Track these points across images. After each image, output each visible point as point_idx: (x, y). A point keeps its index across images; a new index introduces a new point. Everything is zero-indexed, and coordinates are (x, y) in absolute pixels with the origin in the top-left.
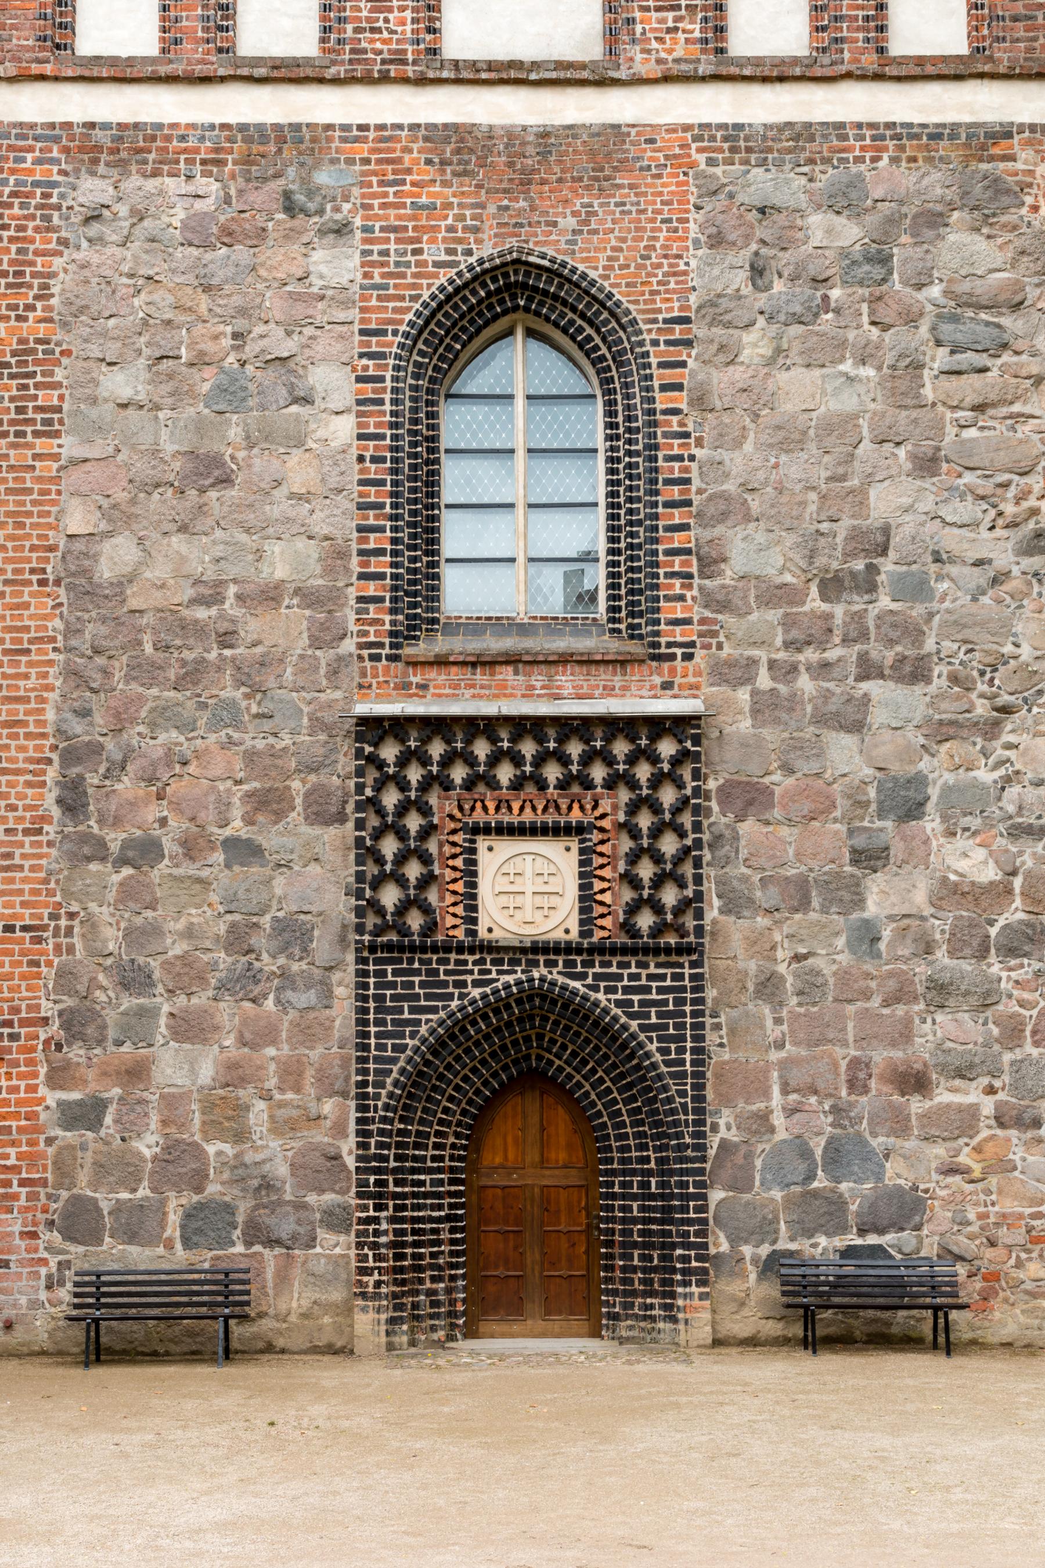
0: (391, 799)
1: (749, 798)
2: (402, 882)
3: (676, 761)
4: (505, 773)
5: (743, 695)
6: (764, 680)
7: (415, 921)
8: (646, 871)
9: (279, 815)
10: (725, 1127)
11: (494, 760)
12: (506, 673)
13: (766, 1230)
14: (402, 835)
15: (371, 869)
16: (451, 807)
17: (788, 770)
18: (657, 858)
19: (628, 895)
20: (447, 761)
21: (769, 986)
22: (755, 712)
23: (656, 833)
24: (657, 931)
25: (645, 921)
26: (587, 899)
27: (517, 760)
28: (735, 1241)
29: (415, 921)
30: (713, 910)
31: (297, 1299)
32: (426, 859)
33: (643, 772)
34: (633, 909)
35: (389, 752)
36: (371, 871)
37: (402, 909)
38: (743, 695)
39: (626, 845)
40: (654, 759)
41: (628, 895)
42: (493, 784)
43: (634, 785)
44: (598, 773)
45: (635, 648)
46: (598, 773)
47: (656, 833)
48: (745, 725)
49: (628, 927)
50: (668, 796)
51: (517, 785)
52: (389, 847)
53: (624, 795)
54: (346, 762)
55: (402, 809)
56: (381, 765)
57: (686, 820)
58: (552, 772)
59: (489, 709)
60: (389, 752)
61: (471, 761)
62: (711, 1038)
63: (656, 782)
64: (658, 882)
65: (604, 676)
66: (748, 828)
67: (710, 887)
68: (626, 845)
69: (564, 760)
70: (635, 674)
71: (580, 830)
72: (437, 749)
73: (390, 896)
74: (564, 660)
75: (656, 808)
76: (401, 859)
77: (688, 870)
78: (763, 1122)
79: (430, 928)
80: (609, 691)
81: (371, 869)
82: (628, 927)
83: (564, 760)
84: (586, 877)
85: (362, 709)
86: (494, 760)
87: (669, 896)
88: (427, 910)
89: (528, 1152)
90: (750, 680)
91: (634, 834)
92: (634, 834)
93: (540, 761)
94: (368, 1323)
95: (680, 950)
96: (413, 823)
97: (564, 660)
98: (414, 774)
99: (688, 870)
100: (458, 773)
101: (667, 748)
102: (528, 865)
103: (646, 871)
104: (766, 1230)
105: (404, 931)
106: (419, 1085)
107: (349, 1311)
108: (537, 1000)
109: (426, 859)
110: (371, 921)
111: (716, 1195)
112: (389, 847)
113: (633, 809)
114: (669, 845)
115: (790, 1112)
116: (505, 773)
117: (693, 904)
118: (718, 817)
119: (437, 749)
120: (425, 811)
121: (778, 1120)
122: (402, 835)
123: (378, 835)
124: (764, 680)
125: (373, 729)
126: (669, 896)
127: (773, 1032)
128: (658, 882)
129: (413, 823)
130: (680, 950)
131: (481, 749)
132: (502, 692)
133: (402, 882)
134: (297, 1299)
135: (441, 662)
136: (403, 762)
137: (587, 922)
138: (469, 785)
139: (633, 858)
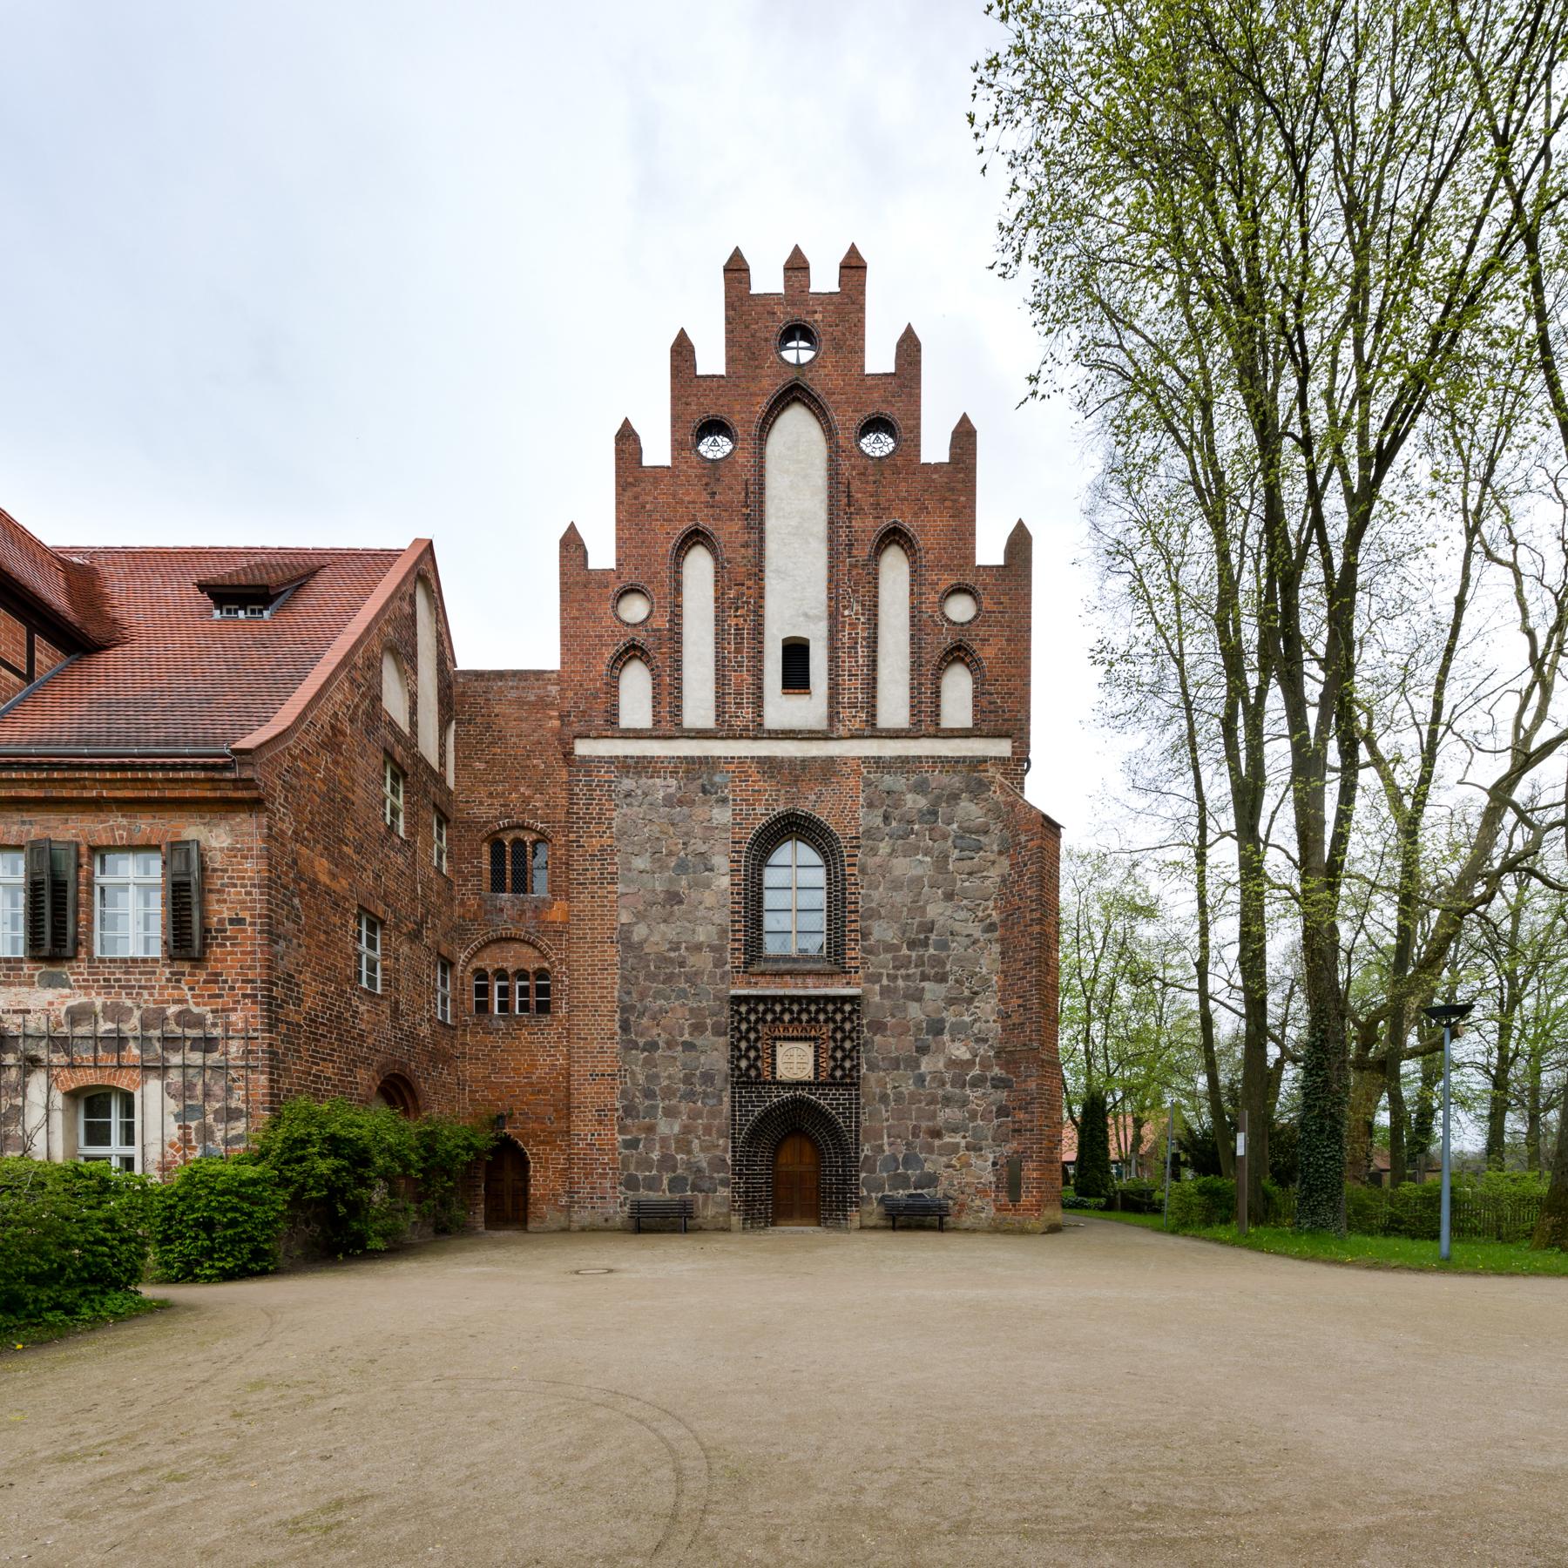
0: (744, 1027)
1: (878, 1027)
2: (748, 1058)
3: (851, 1013)
4: (787, 1017)
5: (877, 987)
6: (885, 982)
7: (753, 1073)
8: (839, 1055)
9: (702, 1033)
10: (866, 1150)
11: (782, 1012)
12: (788, 978)
13: (881, 1188)
14: (748, 1040)
15: (737, 1053)
16: (766, 1030)
17: (893, 1016)
18: (843, 1050)
19: (832, 1064)
20: (765, 1012)
21: (884, 1098)
22: (881, 994)
23: (843, 1040)
24: (843, 1077)
25: (838, 1073)
26: (817, 1065)
27: (791, 1012)
28: (869, 1191)
29: (753, 1073)
30: (864, 1070)
31: (710, 1211)
32: (757, 1050)
33: (839, 1017)
34: (834, 1069)
35: (743, 1009)
36: (736, 1054)
37: (749, 1068)
38: (877, 987)
39: (832, 1044)
40: (843, 1012)
41: (832, 1064)
42: (782, 1021)
43: (835, 1021)
44: (822, 1017)
45: (836, 968)
46: (822, 1017)
47: (843, 1040)
48: (877, 999)
49: (832, 1076)
50: (848, 1026)
51: (791, 1021)
52: (743, 1045)
53: (831, 1026)
54: (727, 1012)
55: (748, 1030)
56: (740, 1013)
57: (854, 1035)
58: (804, 1017)
59: (781, 992)
60: (743, 1009)
61: (774, 1012)
62: (862, 1117)
63: (843, 1020)
64: (843, 1059)
65: (824, 979)
66: (878, 1038)
67: (863, 1061)
68: (832, 1044)
69: (809, 1012)
70: (836, 979)
71: (814, 1039)
72: (761, 1008)
73: (744, 1064)
74: (809, 973)
75: (843, 1031)
76: (748, 1049)
77: (854, 1054)
78: (880, 1149)
79: (759, 1075)
80: (826, 985)
81: (737, 1053)
82: (832, 1076)
83: (809, 1012)
84: (817, 1057)
85: (733, 992)
86: (782, 1012)
87: (847, 1064)
88: (757, 1069)
89: (794, 1158)
90: (879, 981)
91: (835, 1040)
92: (835, 1040)
93: (800, 1012)
94: (735, 1220)
95: (852, 1084)
96: (752, 1036)
97: (809, 973)
98: (753, 1017)
99: (854, 1054)
100: (769, 1017)
101: (848, 1008)
102: (795, 1052)
103: (839, 1055)
104: (881, 1188)
105: (749, 1077)
106: (755, 1135)
107: (729, 1215)
108: (798, 1103)
109: (757, 1050)
110: (737, 1073)
111: (863, 1175)
112: (743, 1045)
113: (834, 1031)
114: (848, 1045)
115: (891, 1144)
116: (787, 1017)
117: (856, 1067)
118: (866, 1033)
119: (761, 1008)
120: (757, 1031)
121: (886, 1147)
122: (748, 1040)
123: (739, 1040)
124: (885, 982)
125: (738, 1000)
126: (847, 1064)
127: (885, 1115)
128: (843, 1059)
129: (752, 1036)
130: (852, 1084)
131: (778, 1008)
132: (786, 986)
133: (748, 1058)
134: (710, 1211)
135: (763, 974)
136: (748, 1012)
137: (817, 1074)
138: (773, 1021)
139: (834, 1050)
